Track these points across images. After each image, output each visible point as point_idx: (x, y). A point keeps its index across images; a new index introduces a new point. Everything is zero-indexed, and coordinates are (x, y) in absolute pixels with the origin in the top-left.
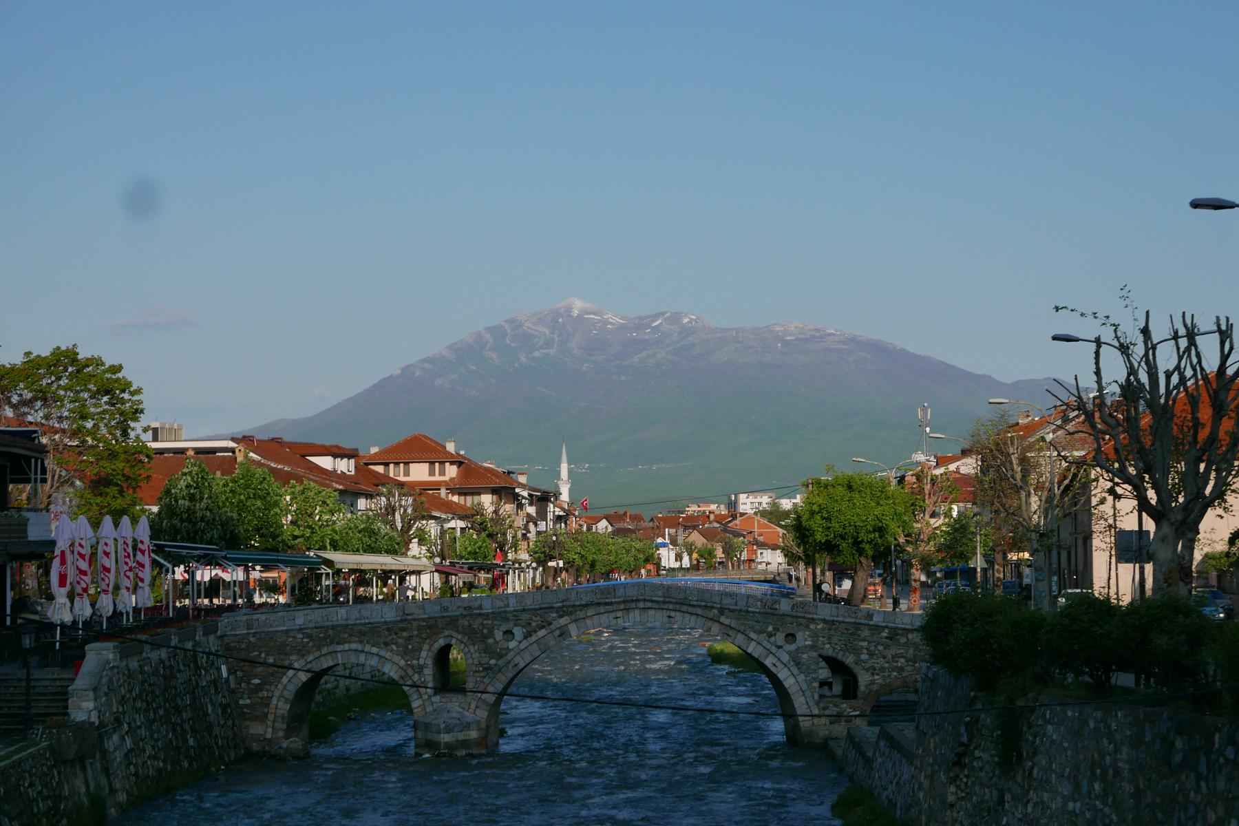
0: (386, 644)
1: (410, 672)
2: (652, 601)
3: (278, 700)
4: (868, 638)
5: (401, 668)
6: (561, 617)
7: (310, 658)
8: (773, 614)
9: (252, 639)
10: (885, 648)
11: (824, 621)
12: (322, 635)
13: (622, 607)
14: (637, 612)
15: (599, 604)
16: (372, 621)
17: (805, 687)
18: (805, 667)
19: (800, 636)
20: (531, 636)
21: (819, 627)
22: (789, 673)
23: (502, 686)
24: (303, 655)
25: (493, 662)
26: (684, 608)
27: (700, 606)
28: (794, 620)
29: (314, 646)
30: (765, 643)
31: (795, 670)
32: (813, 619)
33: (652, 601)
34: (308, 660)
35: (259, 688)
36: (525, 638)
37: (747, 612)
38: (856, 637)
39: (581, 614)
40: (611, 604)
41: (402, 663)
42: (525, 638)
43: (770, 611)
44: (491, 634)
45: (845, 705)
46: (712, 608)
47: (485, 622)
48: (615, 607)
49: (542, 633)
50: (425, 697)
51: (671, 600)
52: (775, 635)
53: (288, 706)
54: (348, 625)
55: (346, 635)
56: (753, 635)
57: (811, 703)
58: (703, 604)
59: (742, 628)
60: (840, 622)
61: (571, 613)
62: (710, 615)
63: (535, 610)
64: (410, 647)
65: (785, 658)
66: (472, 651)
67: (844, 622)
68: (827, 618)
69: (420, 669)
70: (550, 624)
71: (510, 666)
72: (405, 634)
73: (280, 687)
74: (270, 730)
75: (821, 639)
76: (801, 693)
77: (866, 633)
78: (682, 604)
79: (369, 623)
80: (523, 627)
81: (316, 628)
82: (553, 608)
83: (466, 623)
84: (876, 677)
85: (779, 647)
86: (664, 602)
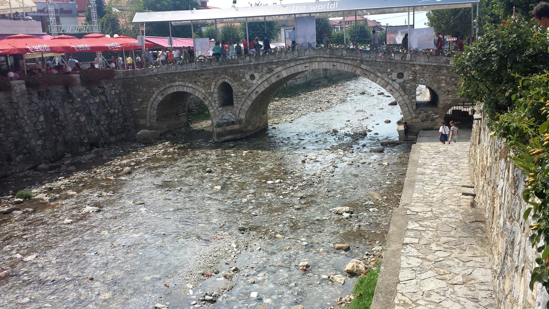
0: (195, 82)
1: (207, 95)
2: (324, 57)
3: (151, 109)
4: (446, 74)
5: (203, 94)
6: (277, 67)
7: (162, 89)
8: (390, 62)
9: (135, 80)
10: (456, 80)
11: (420, 65)
12: (166, 78)
13: (308, 61)
14: (317, 63)
15: (296, 60)
16: (188, 70)
17: (408, 102)
18: (408, 91)
19: (405, 74)
20: (263, 77)
21: (417, 69)
22: (399, 95)
23: (251, 103)
24: (158, 88)
25: (245, 90)
26: (341, 61)
27: (350, 59)
28: (403, 65)
29: (163, 83)
30: (386, 79)
31: (402, 93)
32: (414, 65)
33: (324, 57)
34: (161, 90)
35: (141, 103)
36: (260, 78)
37: (376, 61)
38: (438, 73)
39: (288, 65)
40: (303, 59)
41: (203, 91)
42: (260, 78)
43: (389, 61)
44: (244, 77)
45: (430, 112)
46: (356, 60)
47: (240, 70)
48: (305, 61)
49: (268, 75)
50: (215, 108)
51: (334, 56)
52: (391, 74)
53: (155, 112)
54: (177, 73)
55: (177, 78)
56: (379, 74)
57: (411, 111)
58: (351, 58)
59: (373, 71)
60: (429, 66)
61: (283, 65)
62: (355, 64)
63: (264, 64)
64: (206, 83)
65: (397, 86)
66: (235, 85)
67: (431, 65)
68: (421, 64)
69: (211, 94)
70: (273, 71)
71: (254, 93)
72: (203, 77)
73: (150, 103)
74: (148, 123)
75: (418, 75)
76: (406, 106)
77: (445, 71)
78: (340, 58)
79: (186, 72)
80: (259, 73)
81: (162, 74)
82: (273, 62)
83: (232, 71)
84: (450, 96)
85: (394, 81)
86: (330, 58)
